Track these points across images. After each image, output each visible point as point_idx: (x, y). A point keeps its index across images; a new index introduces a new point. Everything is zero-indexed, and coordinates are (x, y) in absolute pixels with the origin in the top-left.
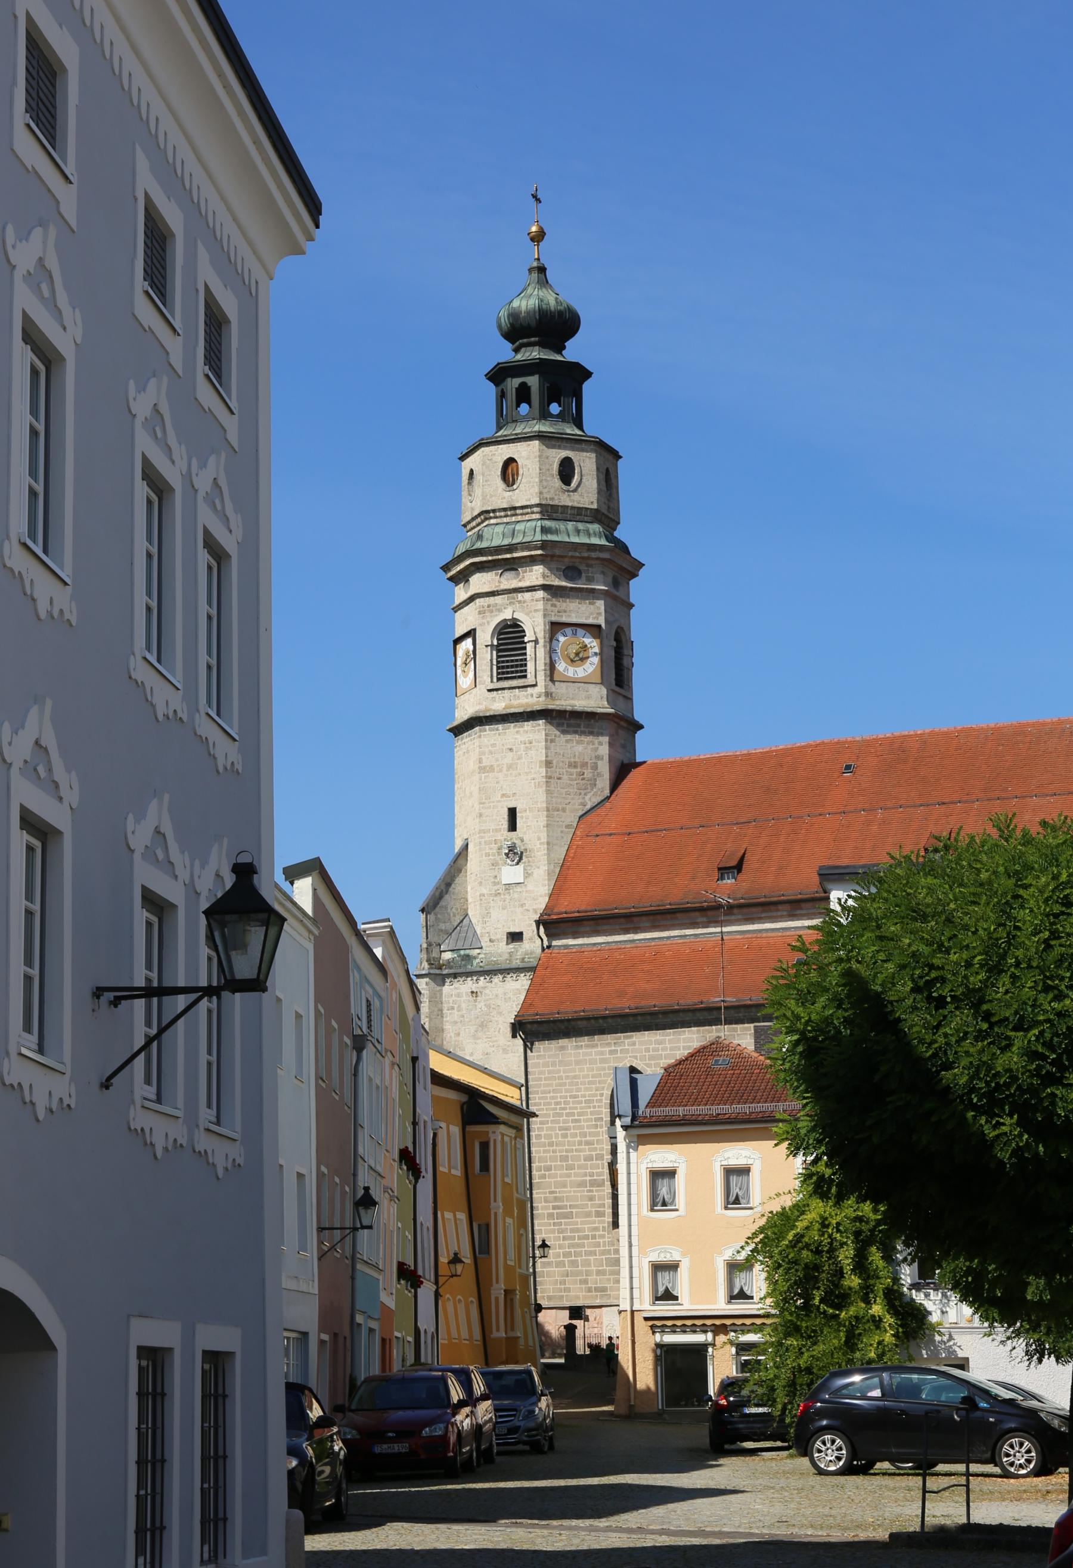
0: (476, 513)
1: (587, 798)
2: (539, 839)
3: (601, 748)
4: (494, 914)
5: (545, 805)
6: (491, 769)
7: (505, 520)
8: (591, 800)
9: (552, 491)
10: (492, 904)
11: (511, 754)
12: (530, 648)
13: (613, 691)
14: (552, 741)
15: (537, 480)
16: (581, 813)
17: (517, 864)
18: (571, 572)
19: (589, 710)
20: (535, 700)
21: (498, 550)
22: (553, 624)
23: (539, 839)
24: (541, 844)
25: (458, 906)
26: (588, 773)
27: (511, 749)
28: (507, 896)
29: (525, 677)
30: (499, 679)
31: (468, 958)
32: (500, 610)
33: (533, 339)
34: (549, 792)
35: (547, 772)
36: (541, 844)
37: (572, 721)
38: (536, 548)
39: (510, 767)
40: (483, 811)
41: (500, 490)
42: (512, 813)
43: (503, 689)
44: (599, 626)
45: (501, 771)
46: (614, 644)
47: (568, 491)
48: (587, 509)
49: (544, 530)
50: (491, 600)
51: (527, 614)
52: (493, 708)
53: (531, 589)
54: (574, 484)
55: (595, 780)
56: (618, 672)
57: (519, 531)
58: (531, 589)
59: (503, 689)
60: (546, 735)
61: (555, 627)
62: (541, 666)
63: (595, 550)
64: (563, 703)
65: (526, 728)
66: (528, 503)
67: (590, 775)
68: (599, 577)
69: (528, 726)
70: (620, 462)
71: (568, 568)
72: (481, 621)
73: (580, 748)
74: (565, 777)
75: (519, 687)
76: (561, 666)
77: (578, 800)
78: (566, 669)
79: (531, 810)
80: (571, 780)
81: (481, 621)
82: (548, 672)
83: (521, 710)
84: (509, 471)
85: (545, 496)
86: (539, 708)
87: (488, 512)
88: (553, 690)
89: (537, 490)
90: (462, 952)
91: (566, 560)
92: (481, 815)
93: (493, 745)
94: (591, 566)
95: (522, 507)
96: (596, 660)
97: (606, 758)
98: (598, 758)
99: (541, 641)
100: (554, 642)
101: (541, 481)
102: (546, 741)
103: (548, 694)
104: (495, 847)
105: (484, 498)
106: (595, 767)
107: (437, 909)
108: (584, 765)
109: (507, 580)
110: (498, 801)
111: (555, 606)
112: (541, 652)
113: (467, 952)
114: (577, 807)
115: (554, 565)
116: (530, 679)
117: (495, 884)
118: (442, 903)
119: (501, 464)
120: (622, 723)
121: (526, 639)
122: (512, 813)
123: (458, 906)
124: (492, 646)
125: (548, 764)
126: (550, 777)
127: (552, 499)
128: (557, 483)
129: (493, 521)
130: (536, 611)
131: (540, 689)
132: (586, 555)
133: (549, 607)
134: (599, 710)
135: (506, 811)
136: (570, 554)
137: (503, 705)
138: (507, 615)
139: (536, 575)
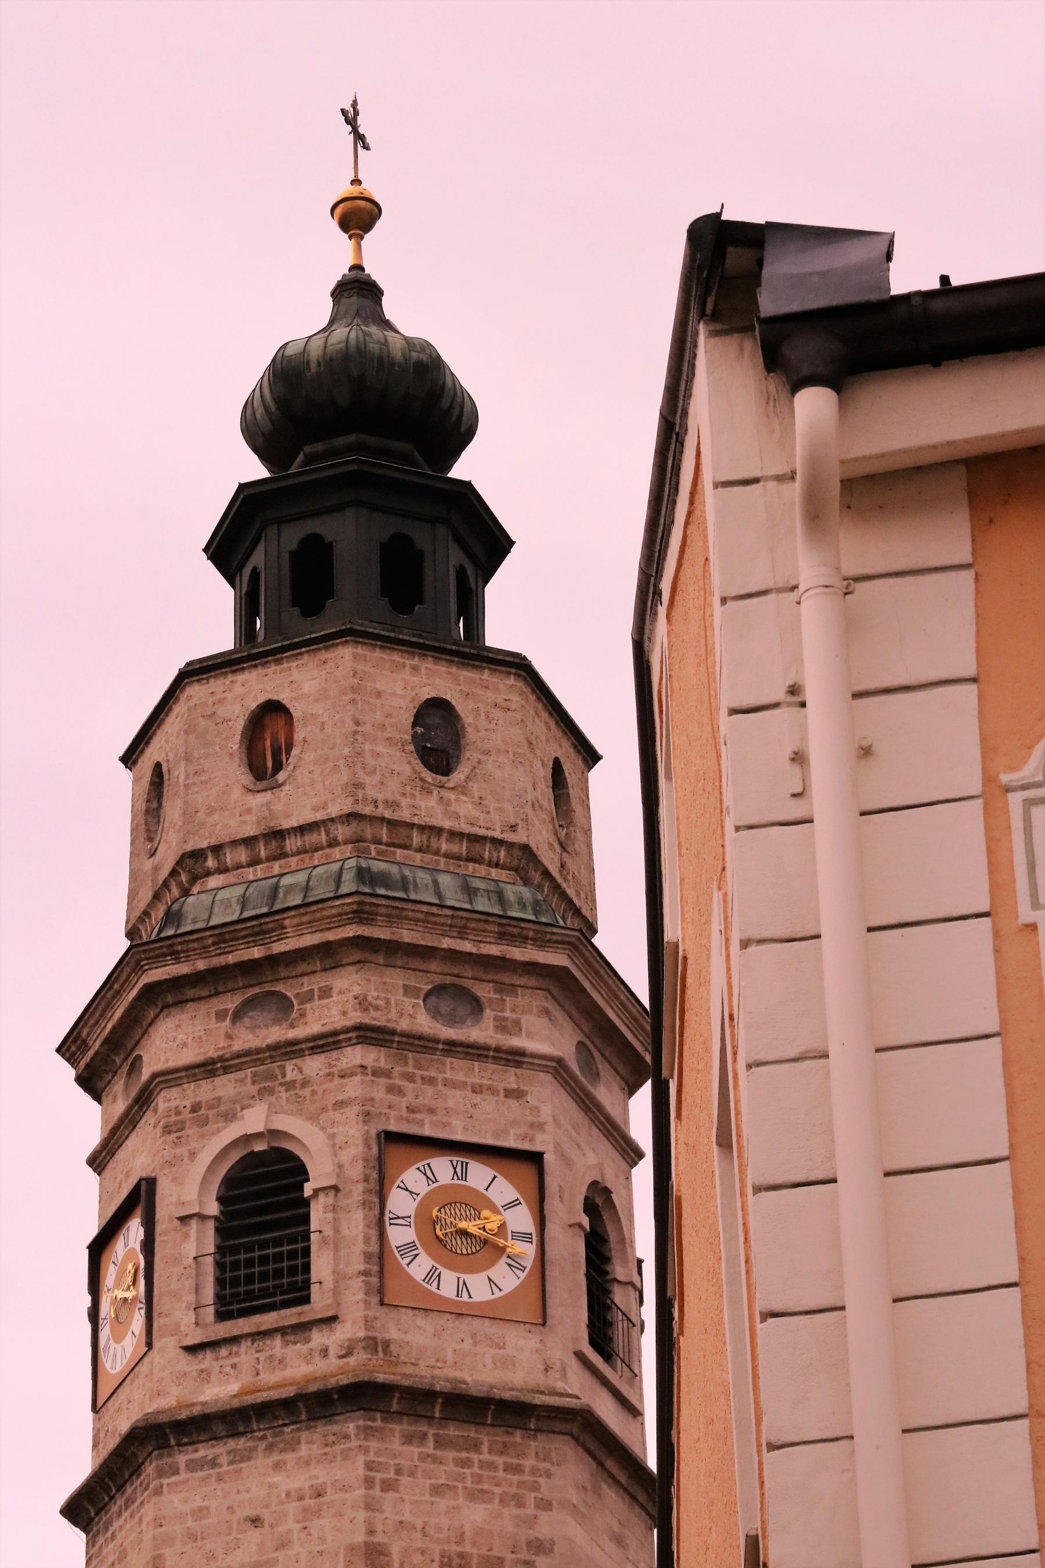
0: (165, 872)
3: (544, 1516)
7: (250, 874)
9: (393, 784)
11: (254, 1535)
13: (580, 1356)
14: (388, 1486)
18: (454, 997)
19: (507, 1395)
20: (333, 1363)
21: (225, 935)
22: (391, 1138)
27: (255, 1521)
29: (306, 1300)
30: (222, 1316)
32: (229, 1117)
33: (341, 441)
37: (453, 1431)
41: (237, 792)
43: (234, 1340)
46: (586, 1221)
48: (497, 842)
49: (362, 874)
50: (203, 1090)
51: (313, 1118)
52: (202, 1398)
53: (327, 1042)
54: (458, 776)
57: (290, 889)
58: (327, 1042)
59: (234, 1340)
60: (369, 1466)
63: (522, 940)
64: (422, 1371)
65: (304, 1451)
66: (320, 816)
68: (532, 1021)
69: (311, 1443)
70: (595, 775)
71: (439, 990)
72: (168, 1154)
73: (475, 1515)
75: (283, 1331)
78: (433, 1275)
83: (289, 1392)
85: (371, 793)
86: (345, 1380)
87: (197, 855)
88: (393, 1334)
93: (201, 1513)
94: (511, 989)
95: (302, 829)
102: (369, 1483)
105: (189, 815)
109: (253, 1029)
111: (401, 1092)
112: (356, 1224)
115: (396, 978)
116: (320, 1302)
119: (240, 724)
120: (610, 1464)
121: (308, 1189)
127: (394, 805)
129: (213, 882)
130: (339, 1105)
132: (494, 950)
133: (379, 1094)
134: (538, 1400)
136: (446, 943)
137: (234, 1388)
138: (254, 1120)
139: (341, 998)
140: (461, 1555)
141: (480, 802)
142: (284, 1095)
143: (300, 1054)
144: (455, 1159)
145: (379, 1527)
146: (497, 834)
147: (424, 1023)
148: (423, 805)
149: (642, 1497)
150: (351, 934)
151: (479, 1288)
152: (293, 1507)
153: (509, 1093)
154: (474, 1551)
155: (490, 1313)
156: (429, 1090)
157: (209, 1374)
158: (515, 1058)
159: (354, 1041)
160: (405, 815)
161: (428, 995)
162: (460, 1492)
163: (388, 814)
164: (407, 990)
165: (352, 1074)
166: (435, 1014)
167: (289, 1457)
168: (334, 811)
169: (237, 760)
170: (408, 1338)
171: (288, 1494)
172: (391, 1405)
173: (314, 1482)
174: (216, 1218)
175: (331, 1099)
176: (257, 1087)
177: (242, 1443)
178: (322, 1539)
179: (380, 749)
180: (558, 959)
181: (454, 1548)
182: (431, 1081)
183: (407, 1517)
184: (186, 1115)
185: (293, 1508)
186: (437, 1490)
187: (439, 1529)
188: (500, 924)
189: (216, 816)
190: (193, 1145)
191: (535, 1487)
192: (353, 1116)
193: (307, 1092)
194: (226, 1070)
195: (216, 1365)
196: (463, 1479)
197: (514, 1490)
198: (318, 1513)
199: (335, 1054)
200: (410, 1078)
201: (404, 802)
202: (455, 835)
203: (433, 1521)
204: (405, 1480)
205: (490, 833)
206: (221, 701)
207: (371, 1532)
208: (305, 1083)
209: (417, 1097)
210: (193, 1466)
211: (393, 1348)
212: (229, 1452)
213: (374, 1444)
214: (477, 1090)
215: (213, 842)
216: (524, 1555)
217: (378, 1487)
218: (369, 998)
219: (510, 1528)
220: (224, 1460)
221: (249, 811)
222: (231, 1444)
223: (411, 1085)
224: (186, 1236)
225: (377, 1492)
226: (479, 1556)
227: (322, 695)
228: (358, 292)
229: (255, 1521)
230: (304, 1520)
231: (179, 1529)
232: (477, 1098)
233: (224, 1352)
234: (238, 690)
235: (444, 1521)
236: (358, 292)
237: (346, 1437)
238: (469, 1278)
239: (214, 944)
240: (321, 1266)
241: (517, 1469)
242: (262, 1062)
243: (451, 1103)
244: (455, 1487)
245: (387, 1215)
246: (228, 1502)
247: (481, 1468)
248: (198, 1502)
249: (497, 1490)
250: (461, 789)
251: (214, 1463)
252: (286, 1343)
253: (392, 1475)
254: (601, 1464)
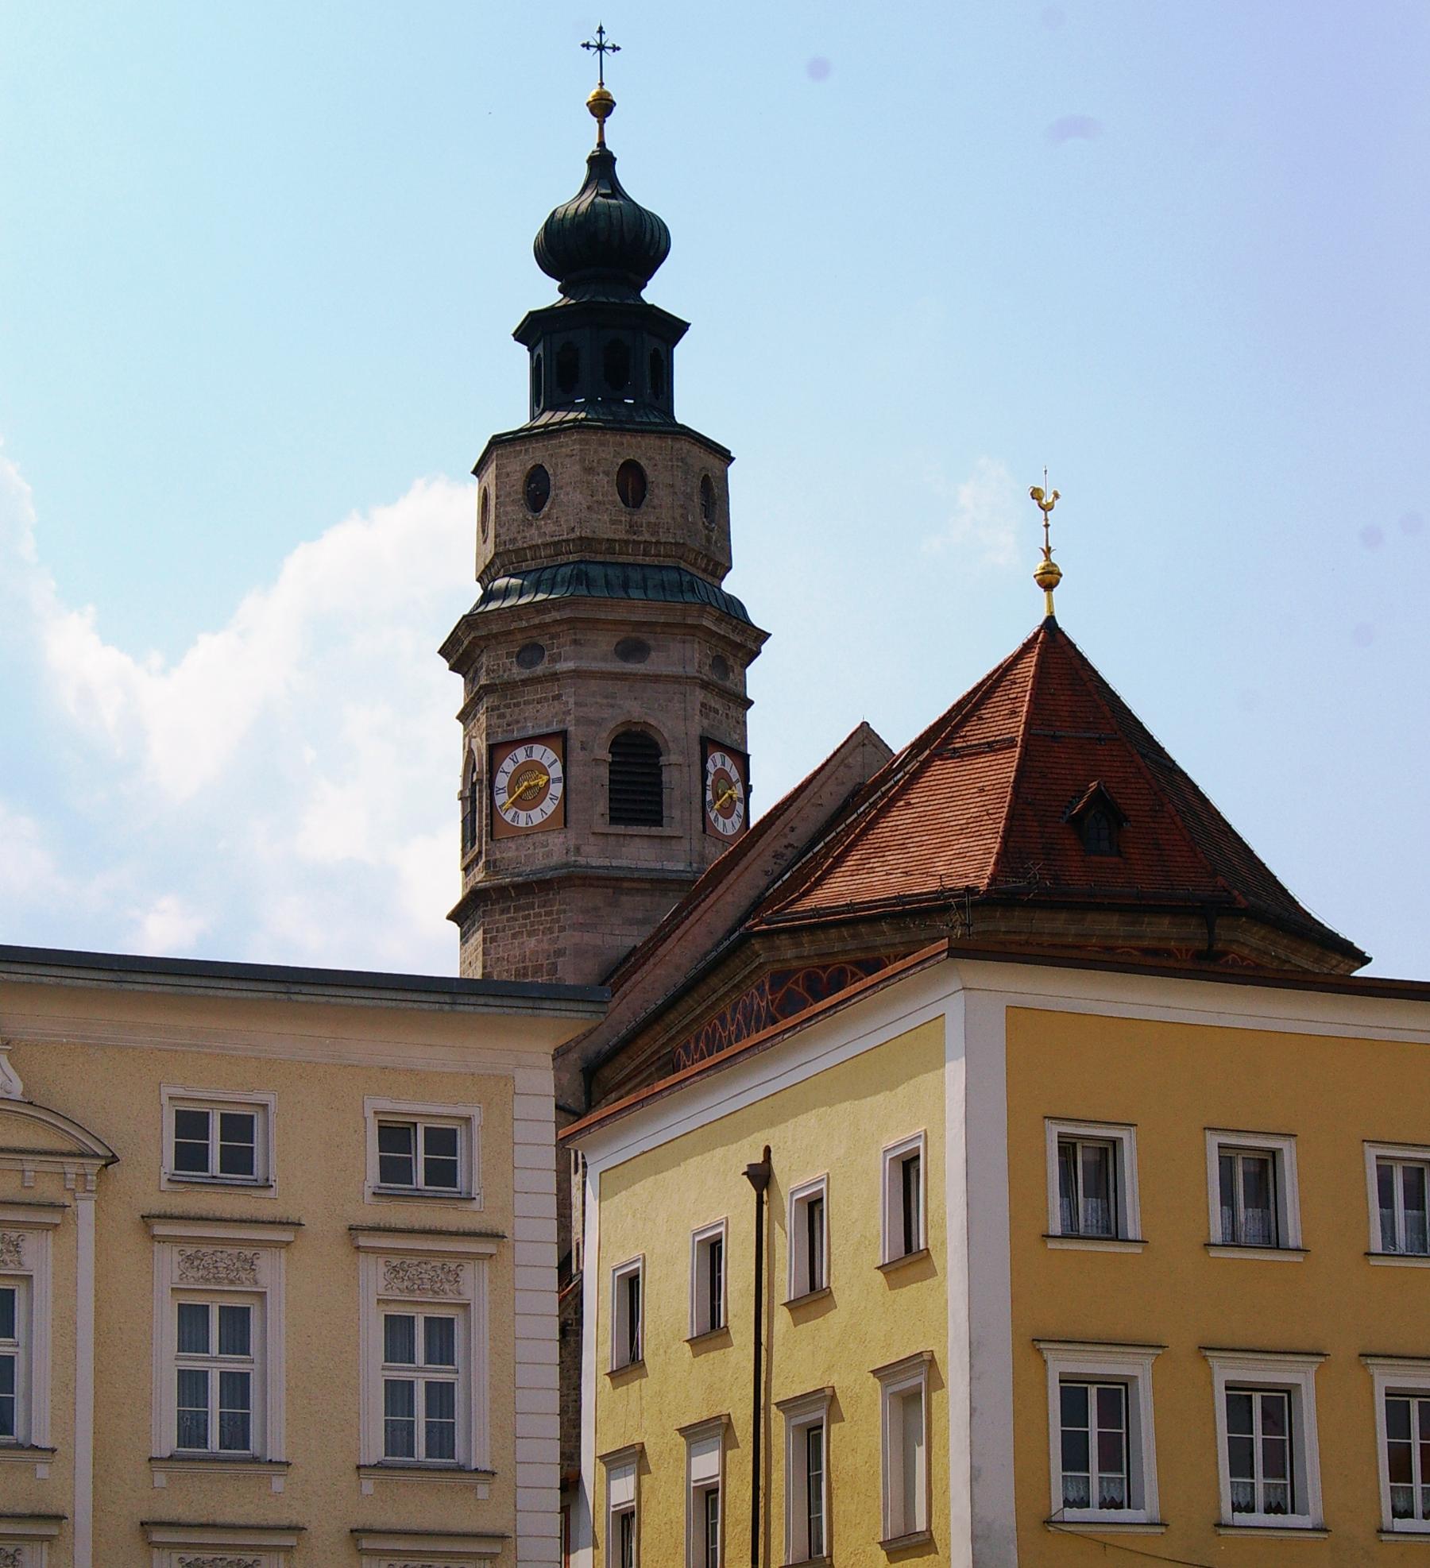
14: (493, 940)
18: (530, 653)
127: (513, 541)
132: (536, 621)
133: (495, 721)
141: (557, 522)
147: (517, 673)
153: (555, 698)
155: (543, 828)
156: (517, 710)
158: (554, 677)
160: (520, 544)
161: (520, 652)
163: (511, 547)
164: (509, 656)
166: (522, 663)
179: (509, 509)
182: (517, 705)
186: (514, 936)
200: (508, 706)
202: (546, 545)
204: (501, 934)
207: (484, 967)
228: (602, 165)
236: (602, 165)
241: (547, 914)
250: (548, 516)
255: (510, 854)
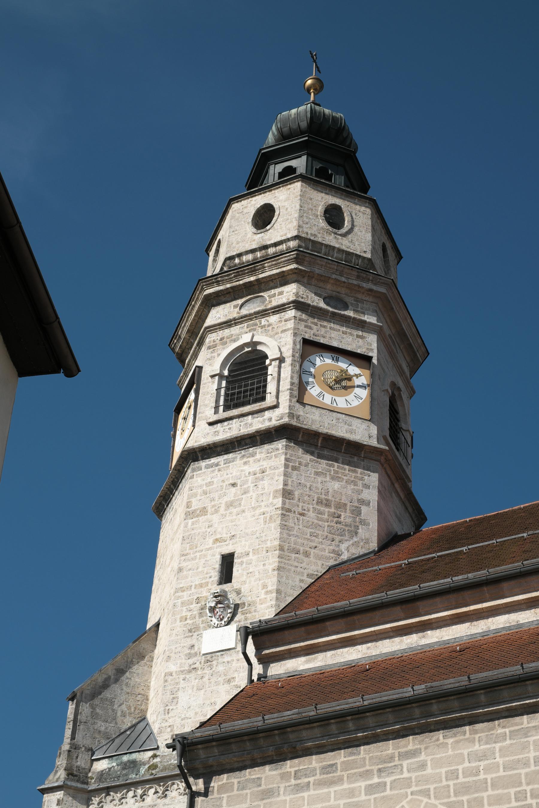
1: (343, 547)
2: (265, 586)
3: (366, 491)
4: (183, 698)
5: (277, 543)
6: (204, 511)
8: (348, 550)
9: (315, 229)
10: (182, 684)
11: (233, 490)
12: (272, 370)
14: (294, 468)
15: (297, 215)
16: (332, 563)
17: (228, 623)
22: (306, 342)
23: (265, 586)
24: (267, 593)
25: (131, 703)
26: (346, 517)
27: (234, 485)
28: (207, 671)
30: (227, 408)
31: (134, 765)
34: (284, 527)
35: (284, 503)
36: (267, 593)
37: (326, 452)
38: (289, 262)
39: (230, 505)
40: (184, 564)
41: (250, 235)
42: (227, 563)
44: (369, 359)
45: (216, 511)
47: (335, 233)
50: (227, 332)
51: (271, 337)
53: (280, 309)
55: (357, 527)
56: (392, 413)
58: (280, 309)
59: (231, 418)
60: (286, 460)
61: (310, 347)
62: (285, 385)
65: (258, 456)
66: (283, 238)
67: (349, 521)
69: (261, 452)
74: (311, 514)
76: (314, 391)
77: (327, 549)
79: (256, 552)
80: (321, 520)
81: (211, 360)
82: (296, 393)
84: (264, 217)
88: (301, 413)
89: (295, 223)
90: (125, 758)
91: (329, 286)
92: (180, 570)
94: (362, 301)
96: (364, 393)
97: (374, 504)
98: (362, 502)
99: (289, 361)
100: (306, 364)
101: (301, 217)
102: (286, 466)
103: (291, 415)
104: (195, 607)
105: (229, 246)
106: (357, 512)
107: (96, 701)
108: (341, 506)
110: (210, 549)
111: (311, 328)
112: (287, 371)
113: (134, 756)
114: (326, 554)
116: (270, 400)
117: (190, 656)
118: (107, 694)
122: (227, 563)
123: (131, 703)
124: (221, 376)
125: (287, 494)
126: (289, 510)
127: (315, 235)
128: (322, 223)
130: (284, 331)
131: (284, 408)
135: (218, 558)
136: (334, 276)
138: (246, 338)
140: (327, 500)
142: (260, 330)
143: (268, 315)
144: (333, 355)
145: (290, 483)
146: (358, 253)
148: (327, 238)
149: (410, 510)
150: (293, 267)
151: (341, 402)
152: (251, 478)
154: (333, 499)
156: (323, 330)
157: (218, 433)
159: (292, 308)
160: (320, 240)
162: (328, 476)
163: (312, 238)
165: (290, 320)
167: (251, 459)
168: (289, 236)
169: (251, 224)
170: (308, 415)
171: (249, 473)
172: (298, 438)
173: (261, 468)
174: (226, 376)
175: (280, 330)
176: (249, 329)
177: (231, 456)
178: (263, 489)
180: (382, 290)
181: (323, 496)
182: (325, 327)
183: (303, 481)
184: (218, 342)
185: (251, 478)
186: (317, 473)
187: (317, 488)
188: (357, 272)
189: (240, 244)
190: (219, 352)
191: (362, 479)
192: (290, 334)
193: (270, 328)
194: (236, 324)
195: (222, 429)
196: (330, 471)
197: (353, 479)
198: (262, 479)
199: (283, 314)
200: (316, 324)
201: (319, 235)
203: (315, 485)
205: (355, 252)
206: (246, 207)
207: (285, 484)
208: (269, 326)
209: (318, 331)
210: (207, 467)
211: (301, 418)
212: (224, 460)
213: (289, 452)
214: (344, 333)
215: (238, 252)
216: (356, 504)
217: (290, 468)
218: (300, 294)
219: (350, 492)
220: (222, 463)
221: (254, 240)
222: (226, 457)
223: (315, 327)
224: (213, 382)
225: (290, 470)
226: (335, 501)
227: (288, 199)
229: (234, 485)
230: (256, 482)
231: (200, 491)
232: (345, 336)
233: (226, 423)
234: (253, 202)
235: (320, 486)
237: (278, 449)
238: (337, 399)
239: (235, 276)
240: (271, 387)
242: (251, 319)
243: (333, 336)
244: (326, 474)
245: (302, 370)
246: (222, 478)
247: (338, 468)
248: (209, 480)
249: (345, 478)
251: (217, 465)
252: (254, 418)
253: (297, 465)
254: (393, 484)
255: (314, 418)
